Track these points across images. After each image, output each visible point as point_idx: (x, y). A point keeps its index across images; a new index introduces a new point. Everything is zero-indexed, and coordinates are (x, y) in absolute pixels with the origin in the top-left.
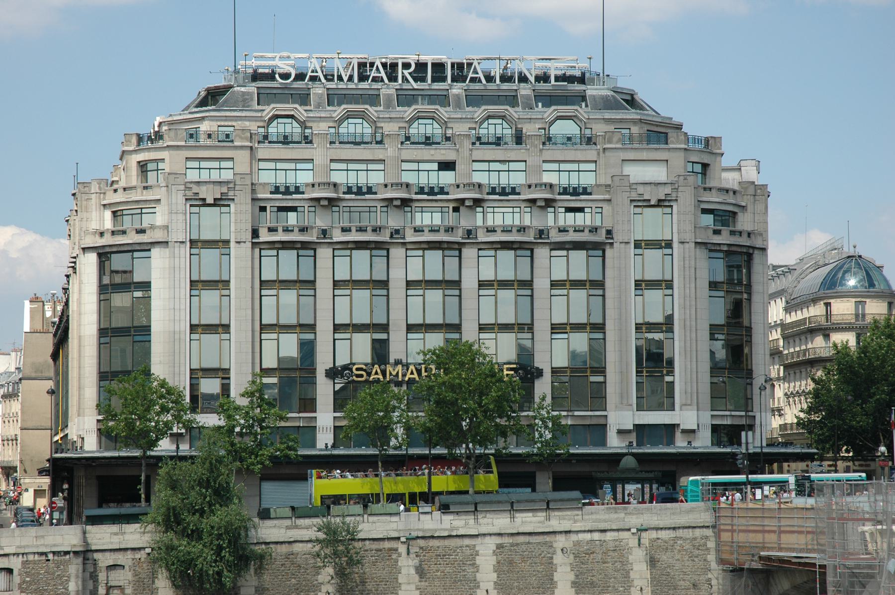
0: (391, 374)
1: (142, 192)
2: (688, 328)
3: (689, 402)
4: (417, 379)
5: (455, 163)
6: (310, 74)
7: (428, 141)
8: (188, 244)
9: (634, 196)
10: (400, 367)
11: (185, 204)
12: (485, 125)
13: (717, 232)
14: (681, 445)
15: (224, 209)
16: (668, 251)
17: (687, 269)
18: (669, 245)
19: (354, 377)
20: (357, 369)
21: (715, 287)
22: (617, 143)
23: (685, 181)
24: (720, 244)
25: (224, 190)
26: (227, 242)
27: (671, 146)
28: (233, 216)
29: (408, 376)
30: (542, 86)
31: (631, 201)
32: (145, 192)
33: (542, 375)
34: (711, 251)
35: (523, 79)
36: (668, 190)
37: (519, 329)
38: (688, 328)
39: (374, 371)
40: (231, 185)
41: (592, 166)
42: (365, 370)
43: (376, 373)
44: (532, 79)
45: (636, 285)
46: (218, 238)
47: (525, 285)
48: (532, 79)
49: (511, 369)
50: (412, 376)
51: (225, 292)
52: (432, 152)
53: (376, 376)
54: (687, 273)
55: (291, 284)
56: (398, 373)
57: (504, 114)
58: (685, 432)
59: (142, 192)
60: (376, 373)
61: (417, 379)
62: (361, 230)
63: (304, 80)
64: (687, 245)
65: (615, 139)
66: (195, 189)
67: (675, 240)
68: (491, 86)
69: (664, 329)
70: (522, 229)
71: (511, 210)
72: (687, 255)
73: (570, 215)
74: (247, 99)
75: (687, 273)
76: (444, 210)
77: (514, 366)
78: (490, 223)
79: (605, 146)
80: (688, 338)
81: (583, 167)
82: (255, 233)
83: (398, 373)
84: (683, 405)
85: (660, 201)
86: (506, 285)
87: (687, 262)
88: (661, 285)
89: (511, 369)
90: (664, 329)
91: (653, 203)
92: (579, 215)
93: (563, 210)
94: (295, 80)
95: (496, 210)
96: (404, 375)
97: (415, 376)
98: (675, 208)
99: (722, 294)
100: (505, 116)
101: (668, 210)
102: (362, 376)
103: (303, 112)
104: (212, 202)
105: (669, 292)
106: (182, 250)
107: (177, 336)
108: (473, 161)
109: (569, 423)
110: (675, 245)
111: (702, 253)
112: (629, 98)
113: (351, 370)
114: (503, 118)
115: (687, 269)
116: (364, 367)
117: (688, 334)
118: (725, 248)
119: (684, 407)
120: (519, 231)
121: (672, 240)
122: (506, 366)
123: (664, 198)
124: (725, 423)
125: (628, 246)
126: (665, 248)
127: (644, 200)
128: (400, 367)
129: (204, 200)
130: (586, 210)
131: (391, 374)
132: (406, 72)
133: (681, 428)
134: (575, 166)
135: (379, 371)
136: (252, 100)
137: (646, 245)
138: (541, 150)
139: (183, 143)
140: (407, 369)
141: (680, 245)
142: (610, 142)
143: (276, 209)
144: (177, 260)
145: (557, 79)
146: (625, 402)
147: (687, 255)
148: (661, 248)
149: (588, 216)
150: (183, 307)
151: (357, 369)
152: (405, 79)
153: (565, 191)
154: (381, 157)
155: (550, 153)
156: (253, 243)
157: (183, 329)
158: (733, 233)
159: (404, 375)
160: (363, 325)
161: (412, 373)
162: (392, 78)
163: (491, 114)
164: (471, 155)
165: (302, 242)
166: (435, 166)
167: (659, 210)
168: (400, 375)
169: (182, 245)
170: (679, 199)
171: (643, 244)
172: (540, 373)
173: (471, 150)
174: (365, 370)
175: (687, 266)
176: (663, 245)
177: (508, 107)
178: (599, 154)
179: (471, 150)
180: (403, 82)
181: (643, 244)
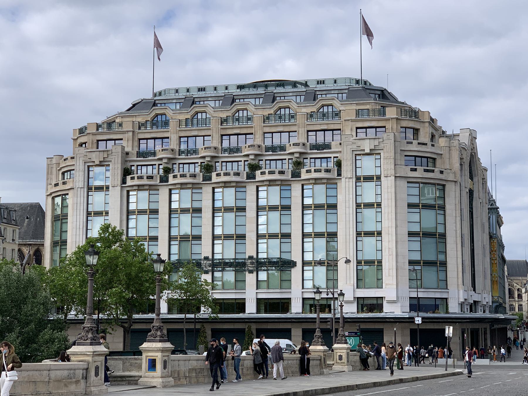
8: (86, 190)
9: (354, 147)
11: (84, 165)
25: (106, 156)
33: (296, 266)
34: (408, 182)
58: (389, 302)
64: (389, 178)
104: (97, 163)
110: (383, 178)
111: (403, 184)
123: (374, 148)
127: (361, 150)
129: (94, 162)
133: (386, 299)
141: (385, 178)
146: (348, 282)
165: (150, 185)
167: (373, 157)
169: (82, 189)
172: (293, 264)
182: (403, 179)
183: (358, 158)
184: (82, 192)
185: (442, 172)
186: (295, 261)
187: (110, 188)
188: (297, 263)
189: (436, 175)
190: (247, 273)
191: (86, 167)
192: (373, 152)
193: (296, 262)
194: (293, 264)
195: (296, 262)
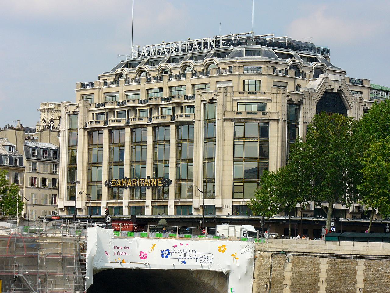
0: (123, 184)
2: (219, 160)
10: (126, 180)
17: (220, 132)
19: (112, 185)
20: (113, 181)
21: (238, 139)
24: (240, 119)
31: (202, 101)
36: (213, 95)
38: (219, 160)
39: (118, 183)
40: (77, 105)
42: (115, 182)
43: (119, 183)
49: (161, 180)
53: (119, 184)
54: (220, 134)
55: (96, 146)
60: (119, 183)
61: (131, 186)
65: (213, 72)
72: (220, 126)
77: (161, 179)
80: (219, 165)
87: (220, 129)
91: (207, 102)
96: (127, 184)
102: (114, 184)
106: (65, 133)
113: (111, 182)
116: (115, 180)
117: (219, 163)
124: (241, 204)
128: (126, 180)
131: (123, 184)
135: (119, 182)
147: (220, 126)
150: (64, 157)
151: (113, 181)
154: (139, 88)
156: (85, 130)
157: (64, 166)
159: (127, 184)
161: (129, 183)
164: (167, 84)
172: (170, 182)
173: (168, 82)
174: (115, 182)
175: (220, 130)
179: (168, 82)
184: (65, 133)
191: (67, 115)
193: (171, 180)
194: (170, 182)
195: (171, 180)
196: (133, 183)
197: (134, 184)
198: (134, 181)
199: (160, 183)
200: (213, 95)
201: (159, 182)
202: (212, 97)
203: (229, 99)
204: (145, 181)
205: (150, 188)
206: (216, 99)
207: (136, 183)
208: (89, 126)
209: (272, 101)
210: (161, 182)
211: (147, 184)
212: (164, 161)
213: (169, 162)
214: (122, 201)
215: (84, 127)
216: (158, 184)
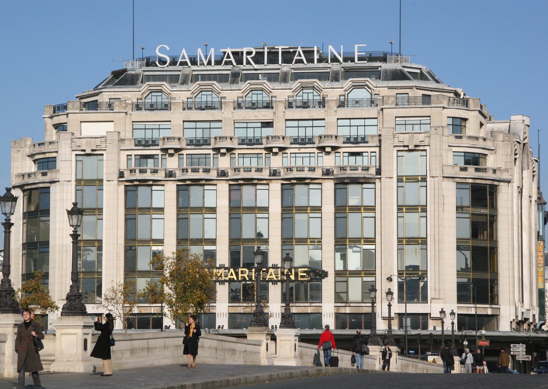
1: (48, 146)
3: (437, 297)
4: (236, 279)
5: (272, 122)
6: (180, 60)
7: (254, 106)
8: (73, 183)
12: (301, 94)
13: (463, 169)
14: (433, 327)
15: (100, 157)
16: (424, 184)
17: (437, 197)
18: (424, 179)
21: (462, 210)
22: (391, 104)
23: (436, 131)
26: (101, 181)
27: (432, 105)
28: (105, 162)
29: (229, 276)
30: (349, 64)
32: (50, 146)
35: (335, 60)
36: (421, 137)
37: (311, 242)
41: (374, 122)
44: (341, 59)
45: (398, 209)
46: (95, 178)
47: (316, 210)
48: (341, 59)
49: (304, 272)
50: (232, 277)
51: (100, 217)
52: (256, 114)
54: (437, 200)
55: (147, 210)
56: (221, 274)
57: (312, 85)
59: (48, 146)
61: (236, 279)
62: (195, 171)
63: (176, 65)
64: (436, 179)
65: (390, 102)
66: (78, 142)
67: (428, 175)
68: (310, 65)
69: (420, 242)
70: (312, 169)
71: (308, 155)
73: (352, 158)
74: (134, 79)
75: (437, 200)
76: (259, 156)
77: (307, 269)
78: (313, 165)
79: (383, 107)
81: (368, 122)
82: (121, 175)
83: (221, 274)
84: (432, 299)
85: (416, 146)
86: (301, 210)
88: (418, 209)
89: (304, 272)
90: (420, 242)
92: (359, 158)
93: (347, 154)
94: (170, 65)
95: (297, 155)
97: (234, 277)
98: (428, 151)
99: (468, 216)
100: (313, 87)
101: (424, 153)
103: (169, 87)
104: (88, 151)
105: (424, 214)
107: (64, 249)
108: (286, 120)
109: (348, 311)
110: (428, 179)
112: (418, 71)
114: (313, 88)
115: (437, 197)
118: (471, 181)
119: (433, 301)
120: (309, 170)
121: (426, 176)
122: (300, 270)
124: (470, 313)
125: (391, 180)
126: (421, 181)
127: (404, 146)
128: (222, 271)
130: (364, 154)
132: (249, 57)
134: (362, 122)
136: (138, 79)
137: (406, 179)
138: (336, 111)
139: (78, 111)
140: (229, 272)
142: (387, 104)
143: (139, 157)
144: (65, 194)
145: (360, 59)
148: (418, 181)
149: (365, 159)
152: (248, 63)
153: (348, 140)
154: (219, 118)
155: (344, 112)
158: (477, 170)
160: (197, 239)
161: (232, 275)
162: (239, 62)
163: (304, 85)
166: (259, 125)
168: (223, 276)
170: (431, 144)
171: (404, 179)
172: (325, 274)
175: (436, 194)
176: (420, 179)
177: (317, 80)
178: (378, 113)
180: (247, 64)
181: (404, 179)
182: (451, 180)
183: (400, 154)
185: (494, 171)
186: (326, 271)
187: (105, 183)
188: (329, 273)
189: (489, 175)
190: (270, 284)
192: (417, 148)
193: (328, 272)
194: (325, 274)
195: (328, 272)
196: (240, 275)
197: (241, 277)
198: (242, 271)
199: (302, 277)
200: (421, 137)
201: (300, 274)
202: (420, 141)
203: (445, 146)
204: (270, 272)
205: (279, 284)
206: (428, 144)
207: (248, 276)
208: (128, 176)
209: (498, 153)
210: (305, 274)
211: (274, 277)
212: (309, 241)
213: (320, 242)
214: (214, 305)
215: (118, 178)
216: (299, 277)
